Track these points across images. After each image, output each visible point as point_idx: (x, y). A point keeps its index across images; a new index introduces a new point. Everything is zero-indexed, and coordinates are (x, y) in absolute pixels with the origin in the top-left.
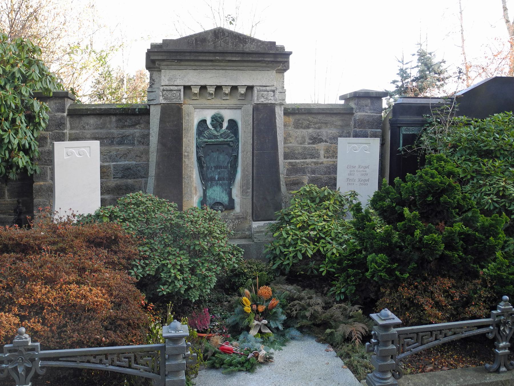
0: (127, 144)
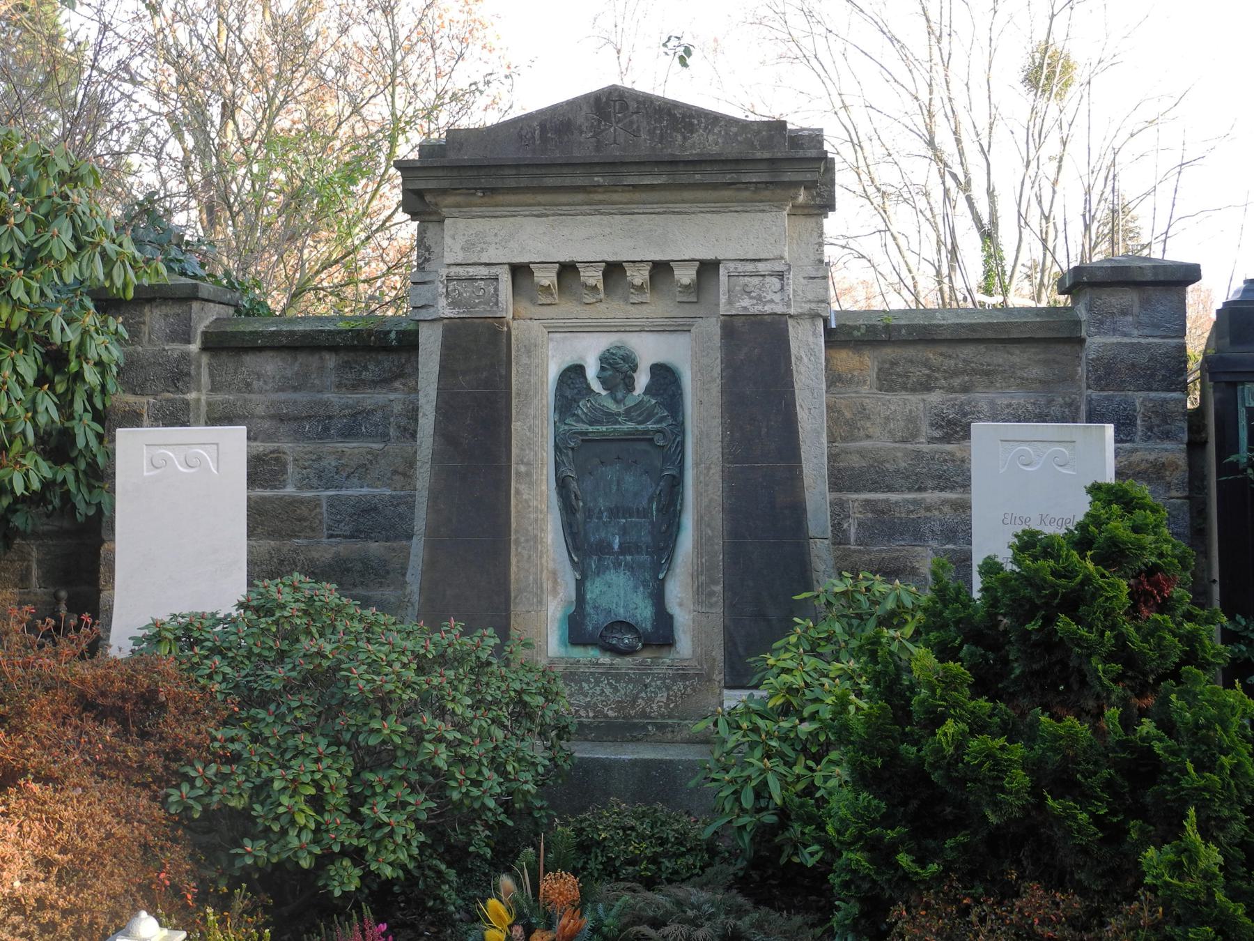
0: (370, 436)
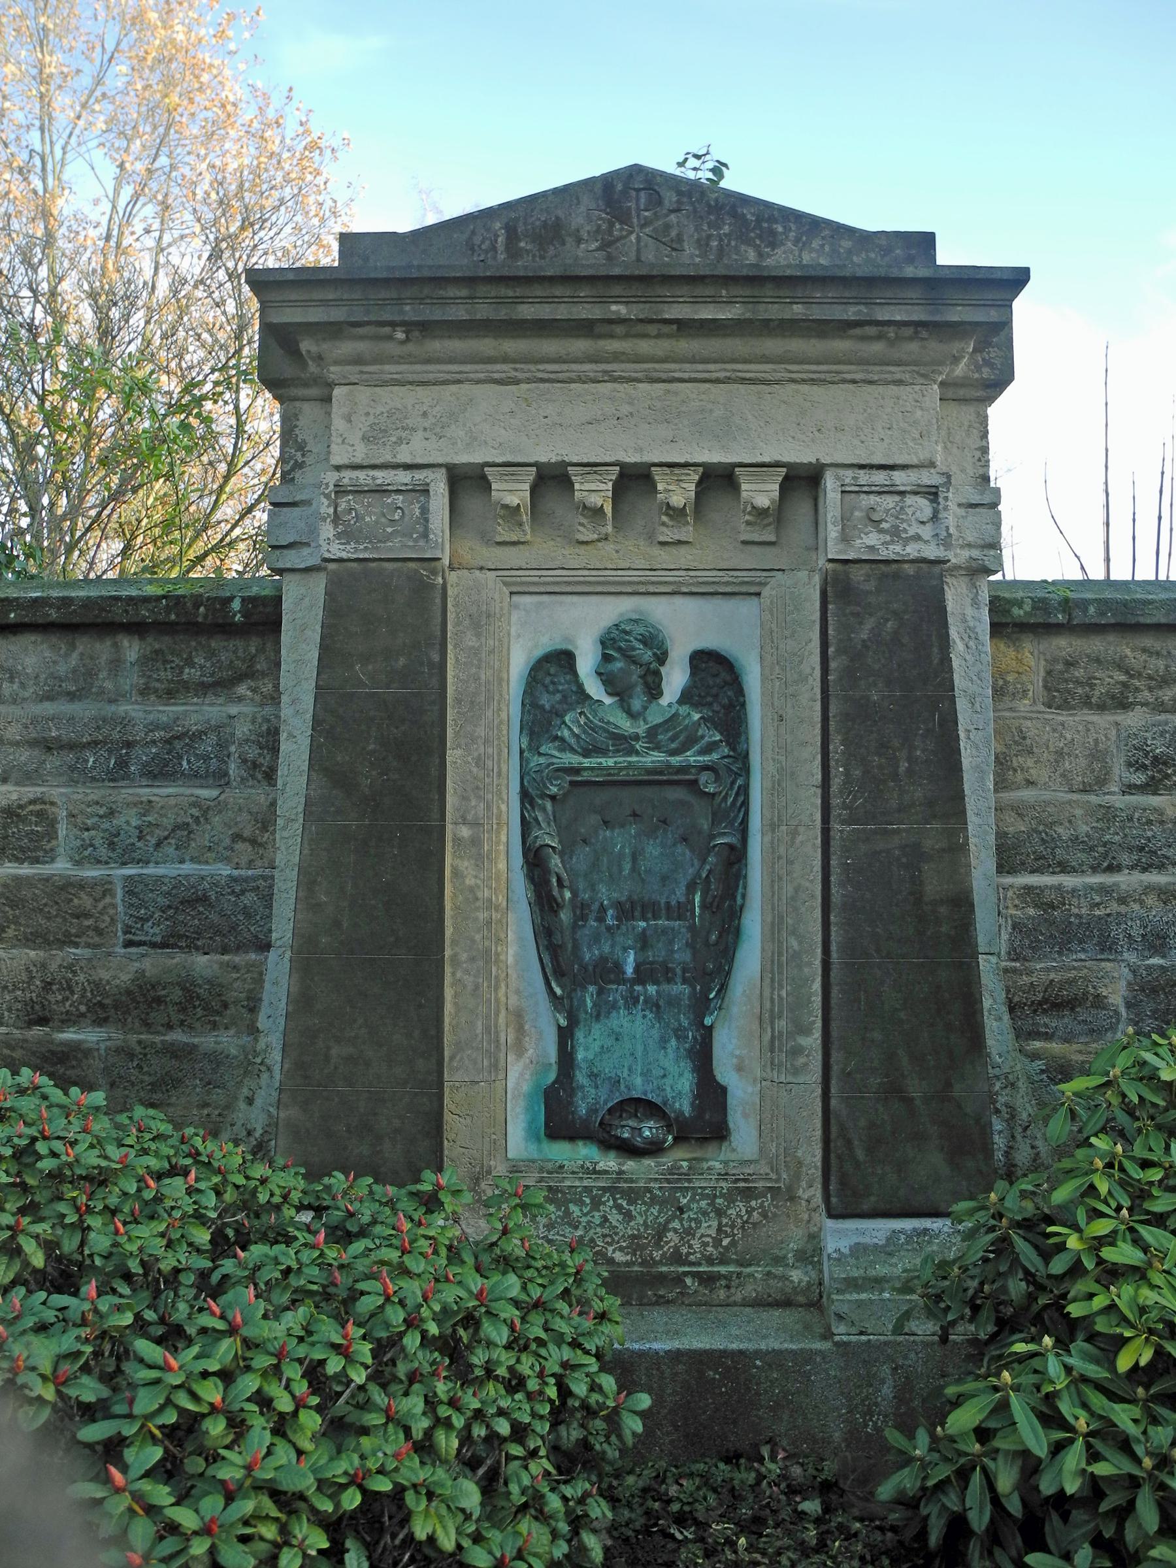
0: (195, 776)
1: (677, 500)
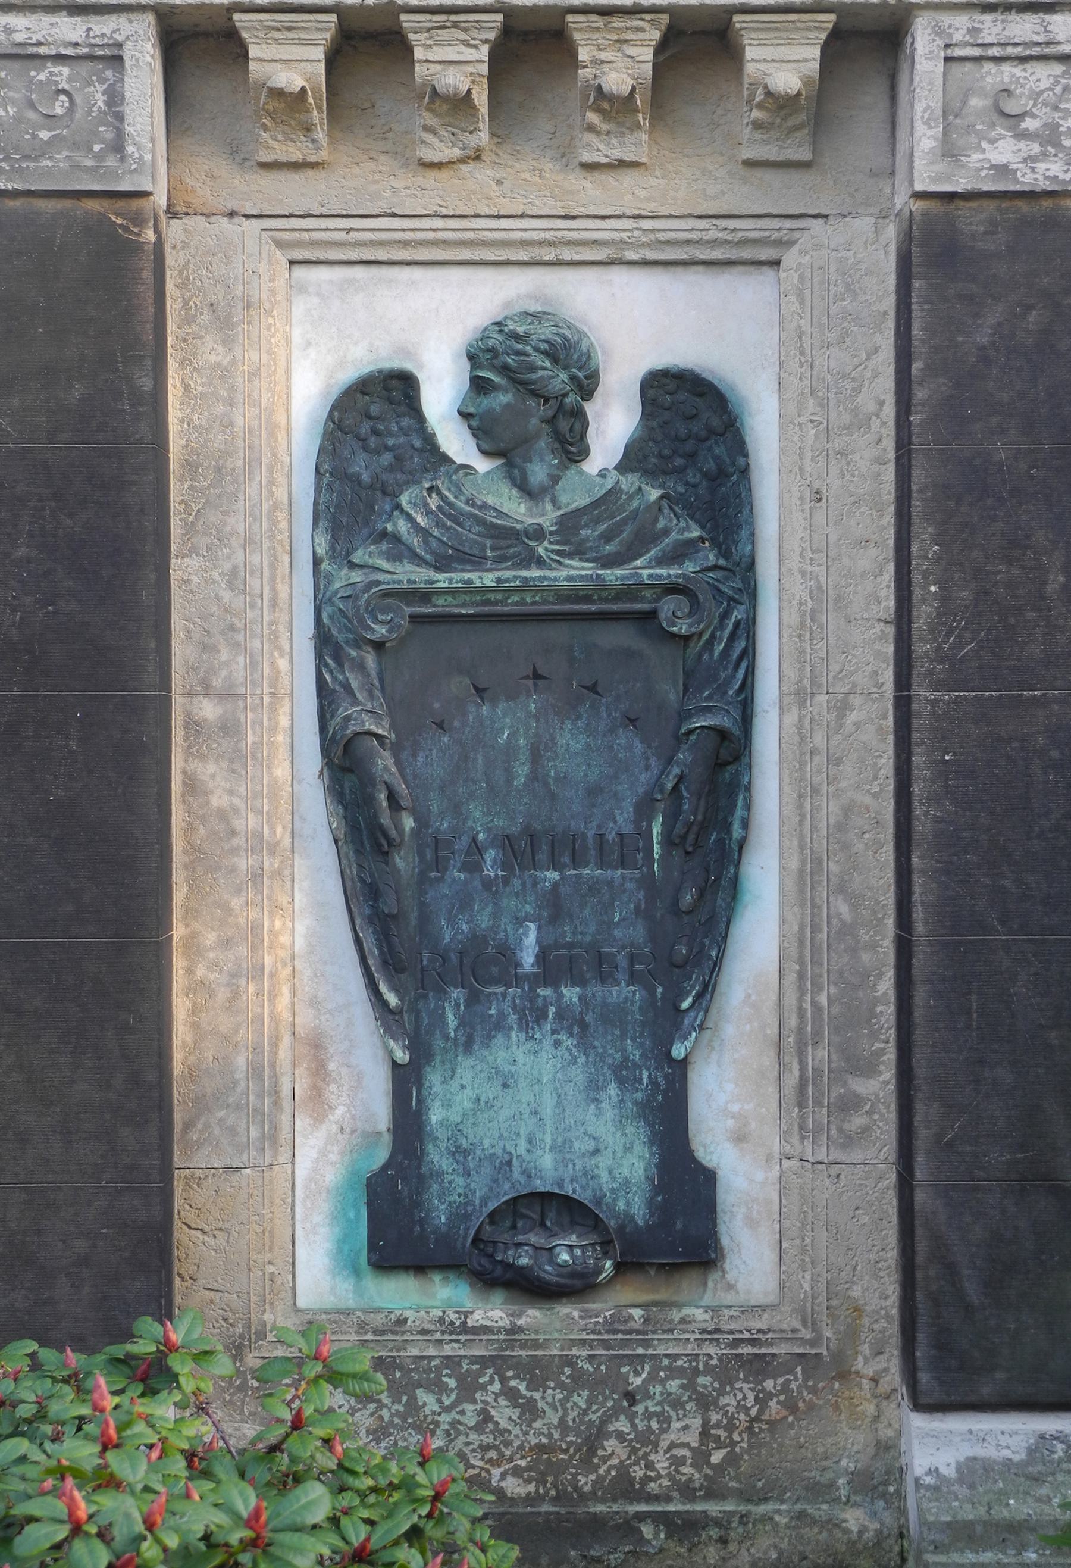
1: (617, 80)
